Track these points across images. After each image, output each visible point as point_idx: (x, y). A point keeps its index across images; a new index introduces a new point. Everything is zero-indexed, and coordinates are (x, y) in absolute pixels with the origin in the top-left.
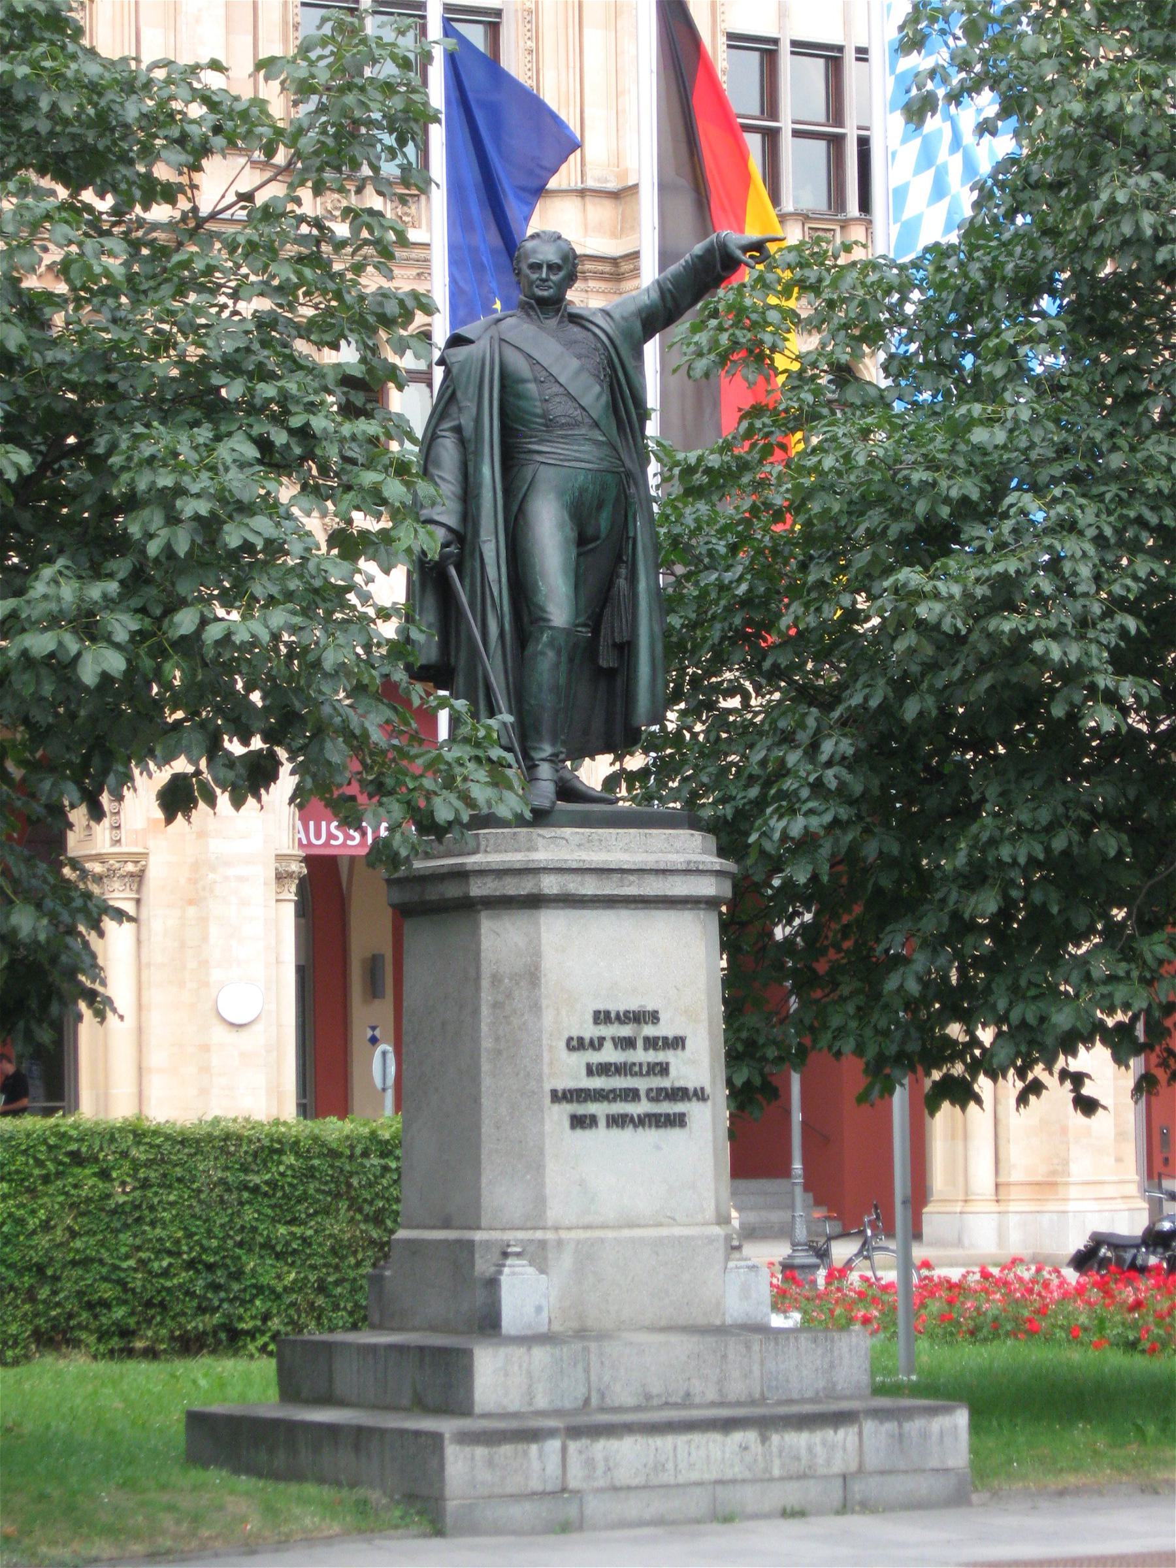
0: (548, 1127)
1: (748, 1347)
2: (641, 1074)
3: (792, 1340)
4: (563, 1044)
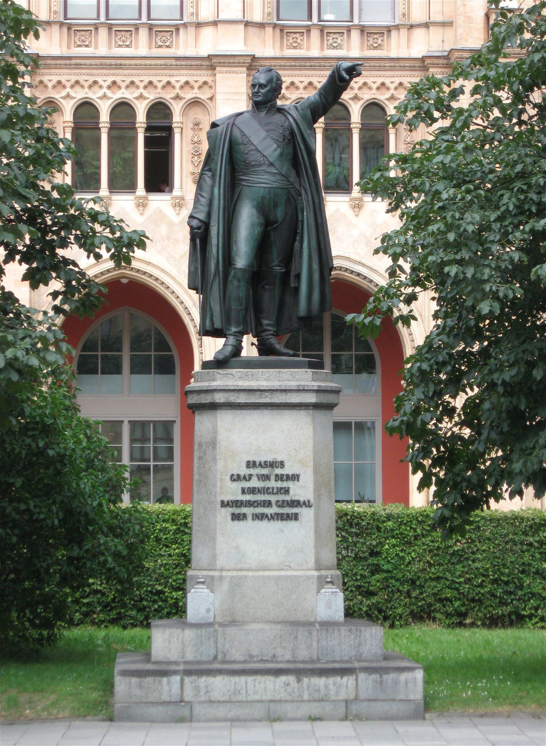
0: (219, 519)
1: (310, 633)
2: (273, 494)
3: (336, 631)
4: (228, 478)
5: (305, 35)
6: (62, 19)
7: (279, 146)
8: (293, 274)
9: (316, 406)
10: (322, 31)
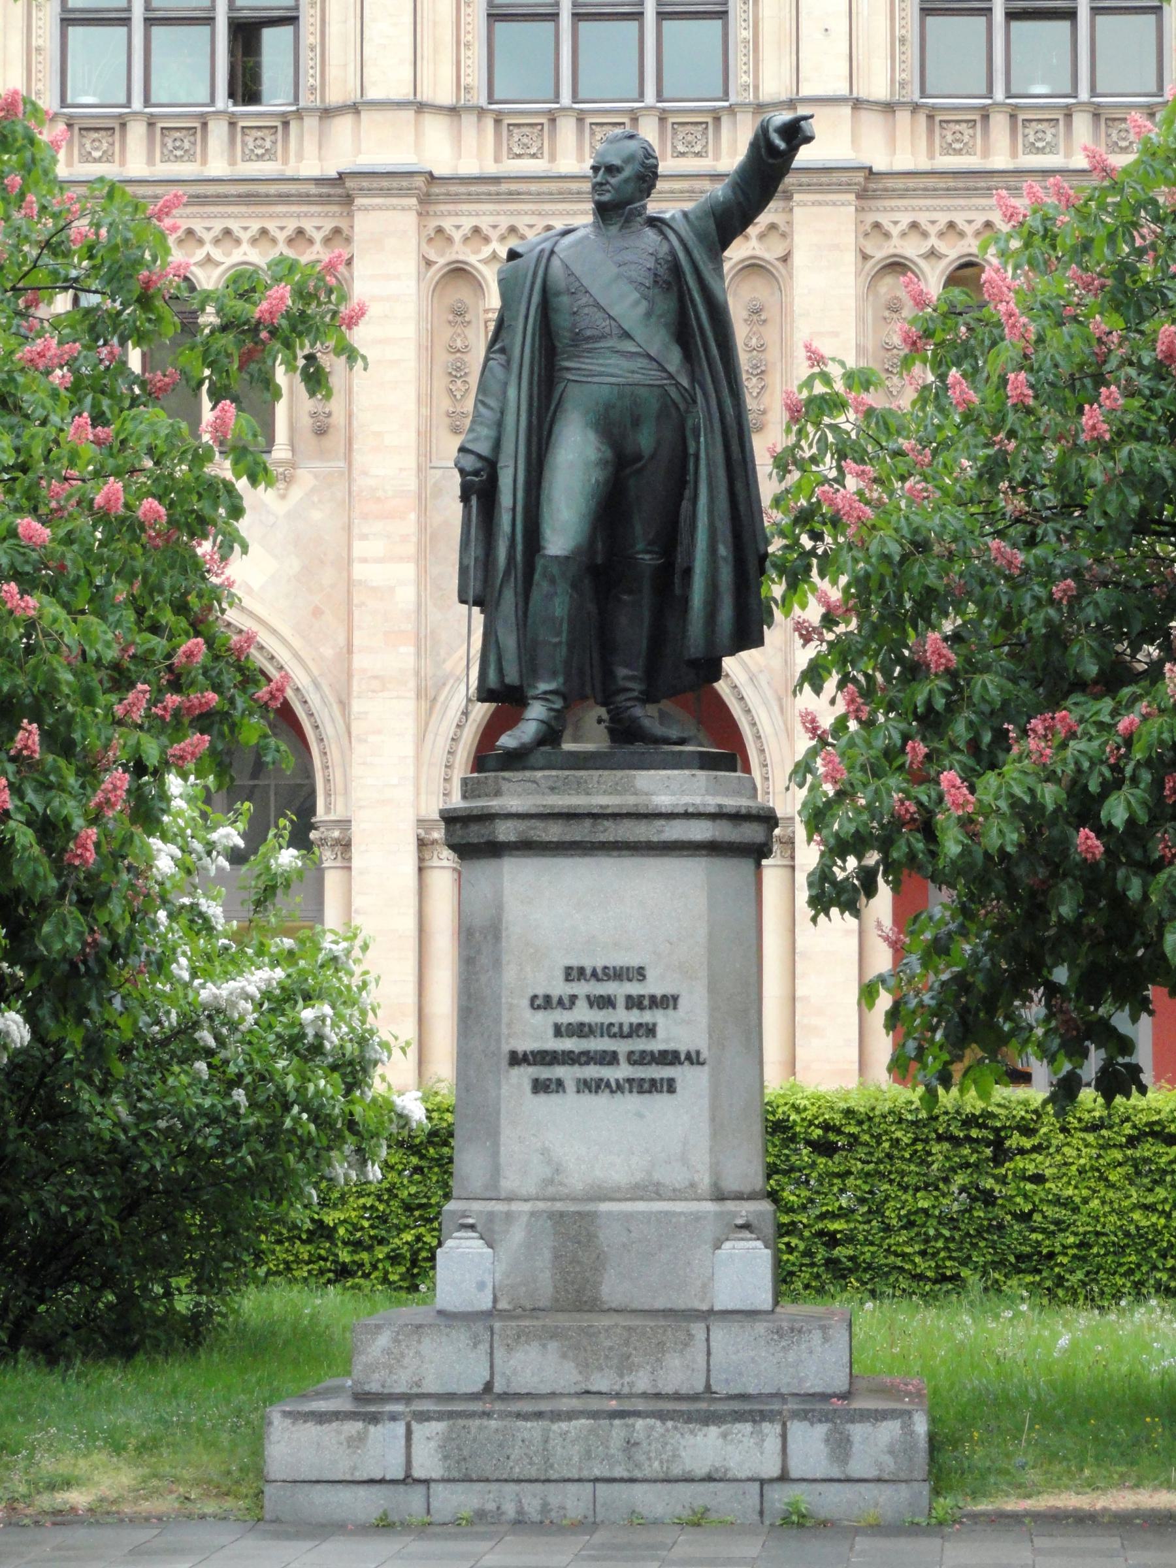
0: (505, 1090)
2: (622, 1036)
4: (526, 1002)
5: (979, 125)
6: (483, 101)
8: (678, 570)
9: (712, 848)
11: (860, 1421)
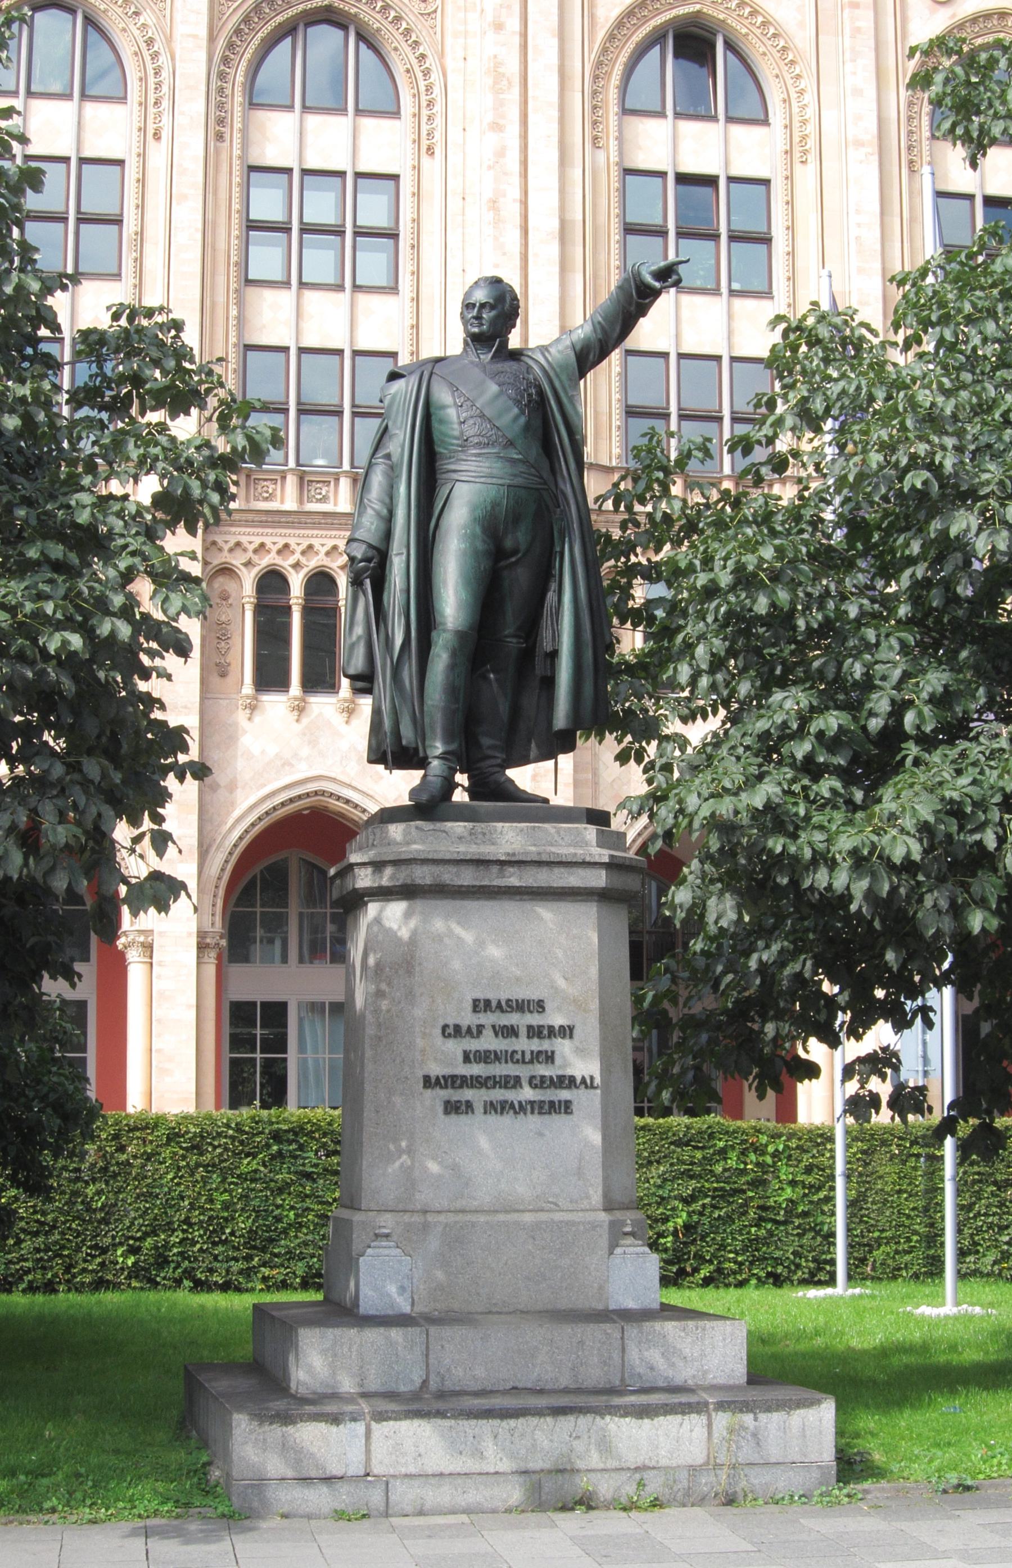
2: (524, 1062)
4: (439, 1031)
7: (522, 412)
10: (301, 479)
11: (777, 1410)
